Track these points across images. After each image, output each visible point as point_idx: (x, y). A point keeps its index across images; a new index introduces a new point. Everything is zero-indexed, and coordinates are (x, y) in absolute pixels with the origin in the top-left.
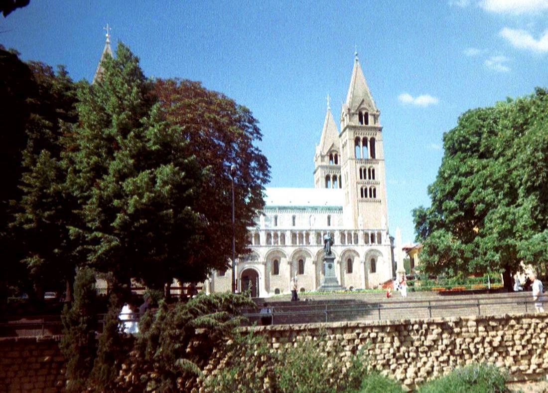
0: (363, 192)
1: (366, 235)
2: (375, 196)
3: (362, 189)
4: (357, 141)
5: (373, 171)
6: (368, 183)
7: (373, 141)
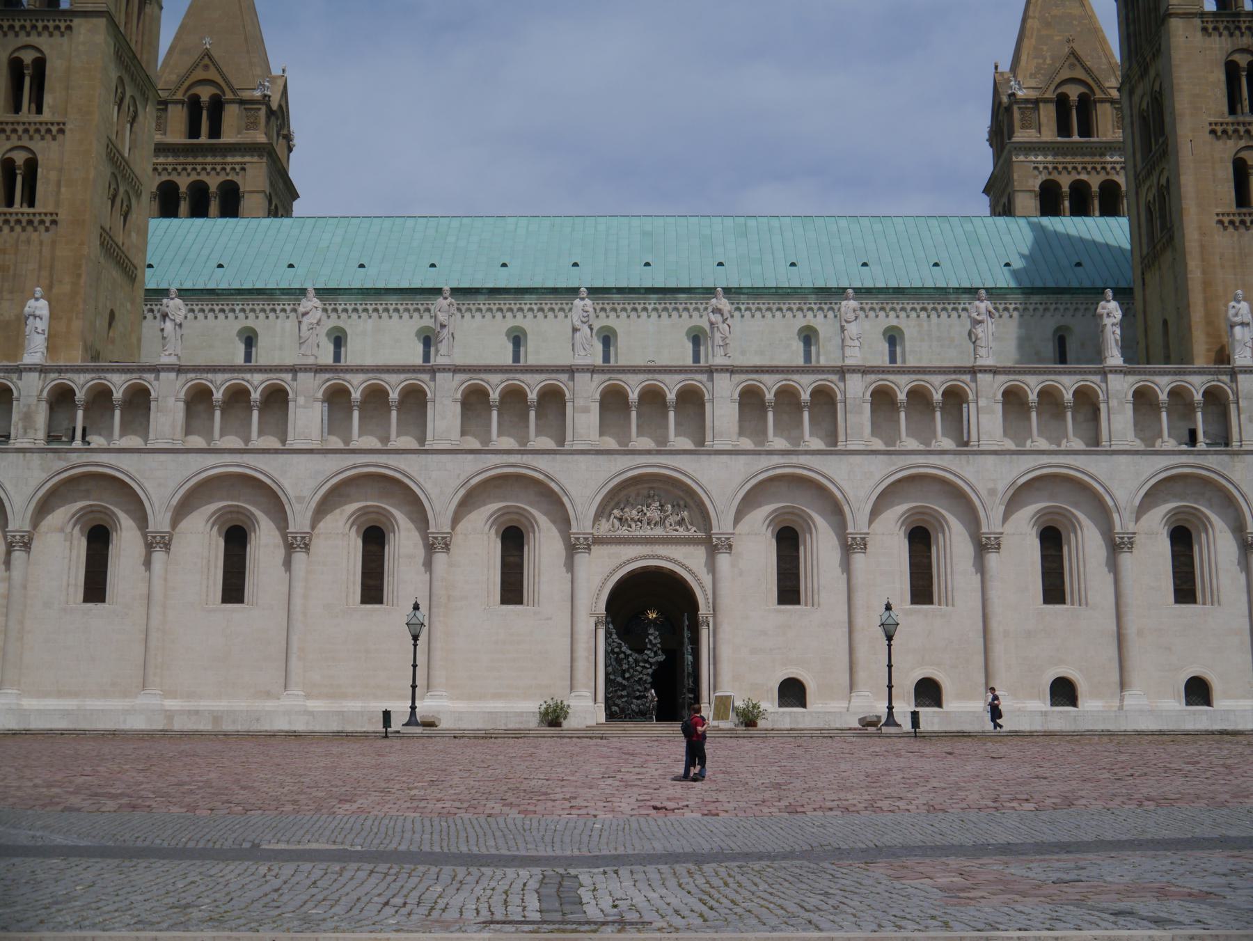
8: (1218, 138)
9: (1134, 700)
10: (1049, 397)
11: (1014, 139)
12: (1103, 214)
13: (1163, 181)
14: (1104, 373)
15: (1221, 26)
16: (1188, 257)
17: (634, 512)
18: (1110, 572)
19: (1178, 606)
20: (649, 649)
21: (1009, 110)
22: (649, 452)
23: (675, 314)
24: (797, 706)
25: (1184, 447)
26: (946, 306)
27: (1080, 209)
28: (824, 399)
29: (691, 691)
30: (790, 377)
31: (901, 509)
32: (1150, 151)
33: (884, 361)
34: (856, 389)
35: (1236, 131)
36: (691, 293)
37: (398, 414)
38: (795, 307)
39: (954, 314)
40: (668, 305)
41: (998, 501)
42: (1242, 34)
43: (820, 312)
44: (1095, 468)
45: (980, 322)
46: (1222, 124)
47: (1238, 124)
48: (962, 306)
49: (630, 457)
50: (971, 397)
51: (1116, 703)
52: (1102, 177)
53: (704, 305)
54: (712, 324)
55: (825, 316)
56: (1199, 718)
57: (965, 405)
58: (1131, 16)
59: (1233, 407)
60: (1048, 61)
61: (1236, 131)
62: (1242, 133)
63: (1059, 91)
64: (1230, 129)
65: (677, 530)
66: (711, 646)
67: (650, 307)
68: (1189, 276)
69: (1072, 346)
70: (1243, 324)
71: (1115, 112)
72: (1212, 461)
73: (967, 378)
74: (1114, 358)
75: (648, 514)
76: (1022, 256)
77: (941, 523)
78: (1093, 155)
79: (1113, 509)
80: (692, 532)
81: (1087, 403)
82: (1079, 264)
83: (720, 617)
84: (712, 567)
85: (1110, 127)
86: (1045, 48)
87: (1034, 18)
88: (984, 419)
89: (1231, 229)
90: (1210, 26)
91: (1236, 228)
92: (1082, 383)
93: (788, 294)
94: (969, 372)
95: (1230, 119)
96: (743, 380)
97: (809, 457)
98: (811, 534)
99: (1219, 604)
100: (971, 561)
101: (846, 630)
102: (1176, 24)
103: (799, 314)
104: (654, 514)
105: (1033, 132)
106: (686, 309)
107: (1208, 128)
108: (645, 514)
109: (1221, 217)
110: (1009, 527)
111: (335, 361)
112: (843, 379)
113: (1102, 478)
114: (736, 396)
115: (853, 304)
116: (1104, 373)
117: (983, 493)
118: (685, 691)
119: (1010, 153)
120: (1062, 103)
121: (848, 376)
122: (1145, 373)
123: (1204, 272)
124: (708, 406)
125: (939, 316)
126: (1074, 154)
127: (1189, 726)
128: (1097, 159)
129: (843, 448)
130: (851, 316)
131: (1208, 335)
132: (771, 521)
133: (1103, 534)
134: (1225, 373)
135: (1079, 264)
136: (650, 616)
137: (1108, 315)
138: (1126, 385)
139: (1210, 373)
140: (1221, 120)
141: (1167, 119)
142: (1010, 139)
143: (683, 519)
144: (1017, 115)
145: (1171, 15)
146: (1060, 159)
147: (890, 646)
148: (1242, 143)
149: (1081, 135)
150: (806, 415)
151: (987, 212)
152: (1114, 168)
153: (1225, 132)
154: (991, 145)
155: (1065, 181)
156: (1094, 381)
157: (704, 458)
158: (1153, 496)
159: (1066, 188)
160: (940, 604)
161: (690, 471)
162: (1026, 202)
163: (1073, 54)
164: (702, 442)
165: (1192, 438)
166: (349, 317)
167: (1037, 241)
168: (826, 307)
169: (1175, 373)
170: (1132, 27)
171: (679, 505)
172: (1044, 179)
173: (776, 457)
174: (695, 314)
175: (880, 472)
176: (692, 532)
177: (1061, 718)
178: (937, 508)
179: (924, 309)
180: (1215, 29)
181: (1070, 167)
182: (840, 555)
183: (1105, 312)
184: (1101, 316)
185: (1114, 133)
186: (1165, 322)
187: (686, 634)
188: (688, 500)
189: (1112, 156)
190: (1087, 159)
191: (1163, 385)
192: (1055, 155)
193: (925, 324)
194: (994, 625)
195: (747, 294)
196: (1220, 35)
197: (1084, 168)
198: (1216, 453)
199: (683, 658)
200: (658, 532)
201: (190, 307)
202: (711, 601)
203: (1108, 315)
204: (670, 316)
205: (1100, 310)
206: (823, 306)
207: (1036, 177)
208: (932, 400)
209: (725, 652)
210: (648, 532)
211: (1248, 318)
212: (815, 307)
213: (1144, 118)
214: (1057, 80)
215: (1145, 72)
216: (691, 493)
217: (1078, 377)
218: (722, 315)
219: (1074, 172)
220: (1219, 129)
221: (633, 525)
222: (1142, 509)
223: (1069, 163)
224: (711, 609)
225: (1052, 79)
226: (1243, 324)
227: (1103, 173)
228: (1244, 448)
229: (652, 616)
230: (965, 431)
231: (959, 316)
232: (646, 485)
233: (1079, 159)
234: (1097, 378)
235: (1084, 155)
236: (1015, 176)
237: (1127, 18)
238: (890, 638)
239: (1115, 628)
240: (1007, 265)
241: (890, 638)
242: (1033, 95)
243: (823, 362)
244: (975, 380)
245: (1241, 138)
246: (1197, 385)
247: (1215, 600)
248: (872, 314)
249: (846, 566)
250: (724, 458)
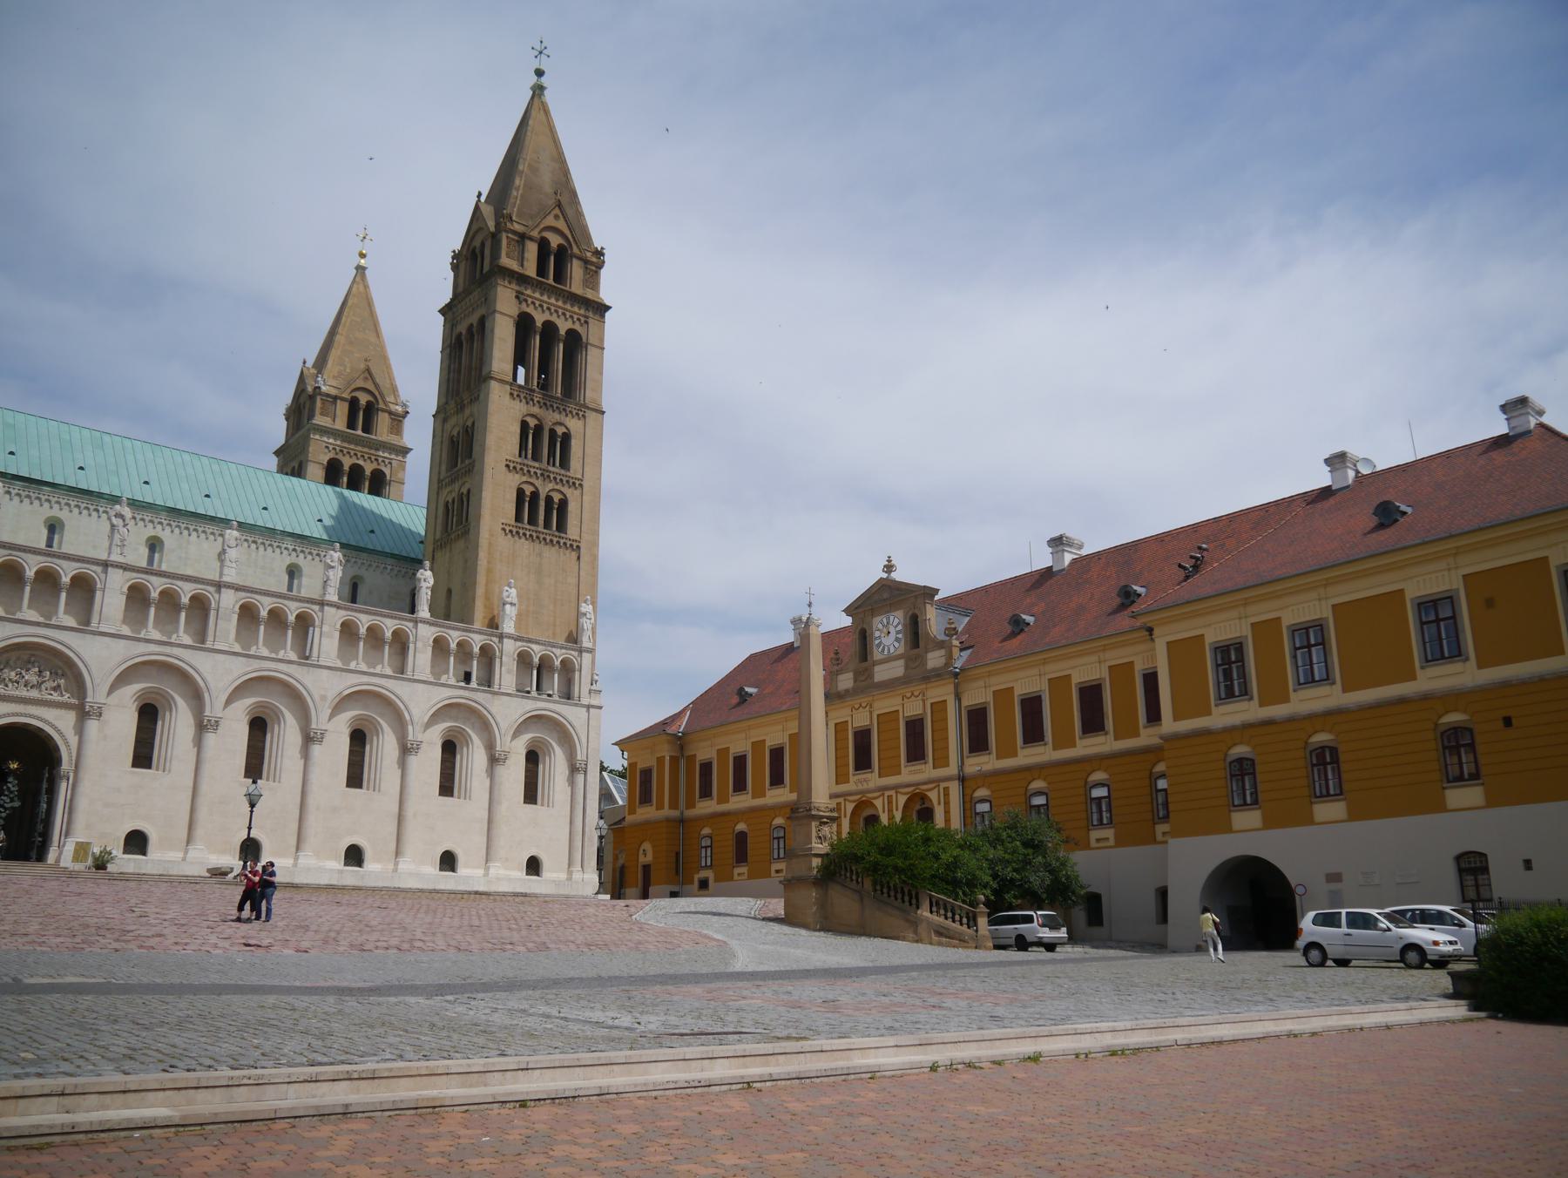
0: (526, 504)
1: (523, 659)
2: (562, 526)
3: (520, 493)
4: (524, 325)
5: (566, 437)
6: (545, 476)
7: (575, 343)
8: (510, 471)
9: (405, 865)
10: (374, 634)
11: (314, 422)
12: (370, 493)
13: (464, 491)
14: (416, 622)
15: (522, 395)
16: (480, 549)
17: (13, 674)
18: (399, 768)
19: (525, 805)
20: (6, 795)
21: (312, 398)
22: (38, 624)
23: (36, 503)
24: (138, 854)
25: (463, 684)
26: (273, 543)
27: (354, 485)
28: (200, 606)
29: (41, 835)
30: (174, 582)
31: (249, 701)
32: (456, 465)
33: (284, 590)
34: (229, 601)
35: (521, 469)
36: (55, 488)
37: (31, 591)
38: (147, 519)
39: (278, 551)
40: (31, 494)
41: (327, 705)
42: (534, 405)
43: (203, 535)
44: (400, 690)
45: (333, 567)
46: (514, 462)
47: (524, 465)
48: (285, 545)
49: (19, 625)
50: (317, 623)
51: (391, 866)
52: (374, 466)
53: (324, 553)
54: (113, 526)
55: (172, 531)
56: (447, 881)
57: (311, 629)
58: (452, 366)
59: (498, 660)
60: (348, 370)
61: (521, 469)
62: (525, 472)
63: (353, 394)
64: (518, 467)
65: (51, 695)
66: (68, 797)
67: (14, 492)
68: (479, 563)
69: (362, 591)
70: (511, 604)
72: (480, 697)
73: (316, 608)
74: (424, 611)
75: (26, 678)
76: (332, 516)
77: (278, 716)
78: (371, 448)
79: (409, 723)
80: (66, 698)
81: (401, 643)
82: (372, 532)
83: (81, 774)
84: (80, 730)
85: (385, 430)
86: (347, 359)
87: (342, 335)
88: (324, 640)
89: (509, 536)
90: (516, 393)
91: (513, 536)
92: (400, 626)
93: (143, 507)
94: (319, 604)
95: (519, 460)
96: (243, 597)
97: (181, 649)
98: (171, 711)
99: (470, 799)
100: (298, 748)
101: (190, 794)
102: (493, 384)
103: (150, 525)
104: (31, 677)
105: (329, 419)
106: (49, 501)
107: (505, 463)
108: (23, 677)
109: (504, 526)
110: (330, 726)
111: (148, 565)
112: (219, 592)
113: (405, 698)
114: (125, 589)
115: (235, 533)
116: (416, 622)
117: (316, 697)
118: (36, 834)
119: (309, 430)
120: (353, 403)
121: (223, 590)
122: (443, 627)
123: (489, 562)
124: (98, 594)
125: (265, 550)
126: (356, 444)
127: (441, 886)
128: (373, 452)
129: (210, 646)
130: (233, 543)
131: (485, 606)
132: (139, 697)
133: (398, 739)
134: (496, 636)
135: (372, 532)
136: (11, 766)
137: (425, 581)
138: (430, 633)
139: (486, 634)
140: (512, 459)
141: (476, 448)
142: (308, 420)
143: (59, 686)
144: (319, 403)
145: (492, 378)
146: (346, 445)
147: (252, 812)
148: (524, 479)
149: (363, 431)
150: (183, 615)
151: (275, 468)
152: (383, 461)
153: (514, 468)
154: (287, 419)
155: (347, 462)
156: (408, 626)
157: (89, 637)
158: (436, 717)
159: (346, 468)
160: (268, 780)
161: (73, 646)
162: (316, 470)
163: (368, 370)
164: (88, 623)
165: (467, 677)
166: (313, 559)
167: (340, 507)
168: (174, 524)
169: (464, 630)
170: (452, 375)
171: (57, 674)
173: (153, 645)
174: (56, 507)
175: (239, 670)
176: (66, 698)
177: (351, 876)
178: (278, 704)
179: (254, 542)
180: (518, 396)
181: (352, 453)
182: (193, 732)
183: (422, 577)
184: (420, 580)
186: (449, 591)
187: (45, 785)
188: (69, 673)
189: (383, 452)
190: (366, 450)
191: (454, 637)
192: (343, 441)
193: (254, 554)
194: (312, 801)
195: (107, 499)
196: (521, 401)
197: (363, 456)
198: (484, 691)
199: (39, 806)
200: (34, 694)
201: (7, 489)
202: (74, 758)
203: (425, 581)
204: (31, 503)
205: (419, 575)
206: (172, 523)
207: (326, 453)
208: (180, 602)
209: (82, 804)
210: (23, 692)
211: (515, 601)
212: (165, 522)
213: (452, 441)
214: (353, 386)
215: (461, 408)
216: (70, 664)
217: (397, 622)
218: (124, 520)
219: (354, 457)
220: (512, 465)
221: (10, 685)
222: (429, 725)
223: (352, 450)
224: (74, 765)
225: (349, 384)
226: (511, 604)
227: (375, 463)
228: (502, 691)
229: (14, 766)
230: (309, 645)
231: (281, 553)
232: (29, 652)
233: (360, 448)
234: (410, 625)
235: (364, 446)
236: (311, 449)
237: (449, 367)
238: (252, 806)
239: (397, 810)
240: (320, 520)
241: (252, 806)
242: (333, 392)
243: (164, 567)
244: (322, 611)
245: (524, 475)
246: (477, 641)
247: (467, 796)
248: (212, 537)
249: (198, 742)
250: (107, 639)
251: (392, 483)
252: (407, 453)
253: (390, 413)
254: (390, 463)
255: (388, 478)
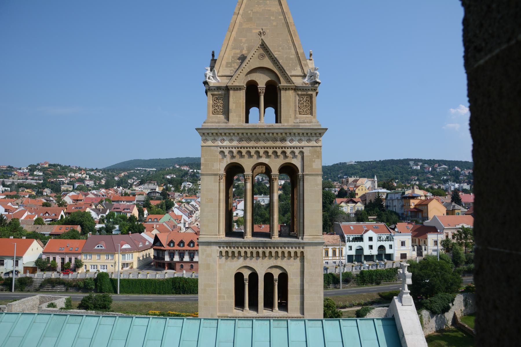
71: (298, 98)
78: (275, 140)
85: (292, 113)
126: (258, 140)
128: (278, 144)
146: (244, 144)
163: (263, 46)
172: (229, 162)
181: (253, 151)
185: (296, 118)
189: (292, 141)
190: (270, 144)
233: (262, 144)
242: (223, 82)
251: (305, 177)
252: (321, 135)
253: (296, 89)
254: (302, 153)
255: (300, 173)
